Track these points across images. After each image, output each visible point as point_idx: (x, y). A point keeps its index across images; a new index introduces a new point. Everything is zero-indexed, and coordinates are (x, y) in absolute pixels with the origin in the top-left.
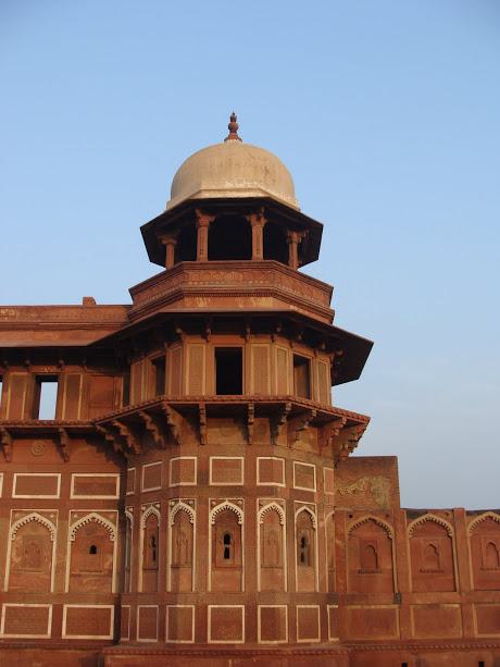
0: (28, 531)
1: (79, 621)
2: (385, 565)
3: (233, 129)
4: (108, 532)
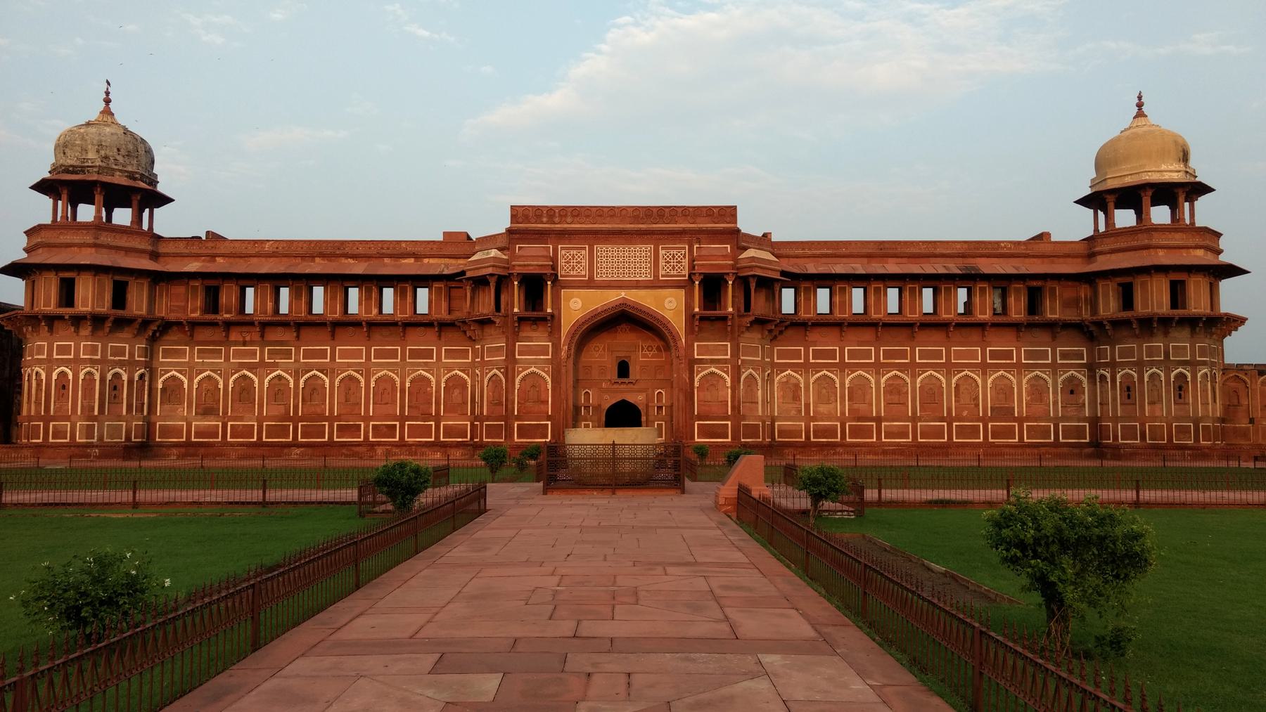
0: (1033, 382)
1: (1068, 432)
3: (1140, 105)
4: (1081, 382)
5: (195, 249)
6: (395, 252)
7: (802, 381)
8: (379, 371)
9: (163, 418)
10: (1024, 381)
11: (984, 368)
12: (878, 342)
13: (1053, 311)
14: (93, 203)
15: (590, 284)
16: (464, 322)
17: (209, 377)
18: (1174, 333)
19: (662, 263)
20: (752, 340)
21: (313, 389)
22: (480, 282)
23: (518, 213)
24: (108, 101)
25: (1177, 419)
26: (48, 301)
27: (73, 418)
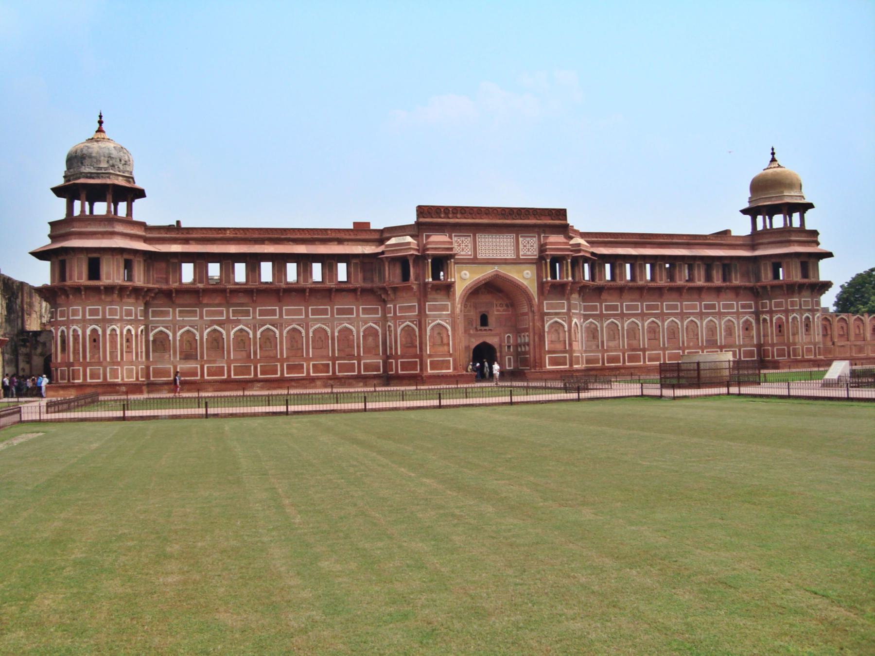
1: (747, 354)
2: (829, 333)
3: (773, 154)
4: (751, 323)
5: (174, 235)
6: (324, 237)
7: (599, 325)
8: (315, 325)
9: (155, 362)
11: (701, 315)
12: (641, 298)
13: (736, 280)
14: (104, 201)
15: (474, 261)
16: (384, 289)
17: (188, 331)
18: (804, 293)
19: (521, 246)
20: (575, 298)
21: (268, 339)
22: (393, 260)
23: (422, 211)
24: (100, 122)
25: (806, 344)
26: (79, 275)
27: (104, 364)
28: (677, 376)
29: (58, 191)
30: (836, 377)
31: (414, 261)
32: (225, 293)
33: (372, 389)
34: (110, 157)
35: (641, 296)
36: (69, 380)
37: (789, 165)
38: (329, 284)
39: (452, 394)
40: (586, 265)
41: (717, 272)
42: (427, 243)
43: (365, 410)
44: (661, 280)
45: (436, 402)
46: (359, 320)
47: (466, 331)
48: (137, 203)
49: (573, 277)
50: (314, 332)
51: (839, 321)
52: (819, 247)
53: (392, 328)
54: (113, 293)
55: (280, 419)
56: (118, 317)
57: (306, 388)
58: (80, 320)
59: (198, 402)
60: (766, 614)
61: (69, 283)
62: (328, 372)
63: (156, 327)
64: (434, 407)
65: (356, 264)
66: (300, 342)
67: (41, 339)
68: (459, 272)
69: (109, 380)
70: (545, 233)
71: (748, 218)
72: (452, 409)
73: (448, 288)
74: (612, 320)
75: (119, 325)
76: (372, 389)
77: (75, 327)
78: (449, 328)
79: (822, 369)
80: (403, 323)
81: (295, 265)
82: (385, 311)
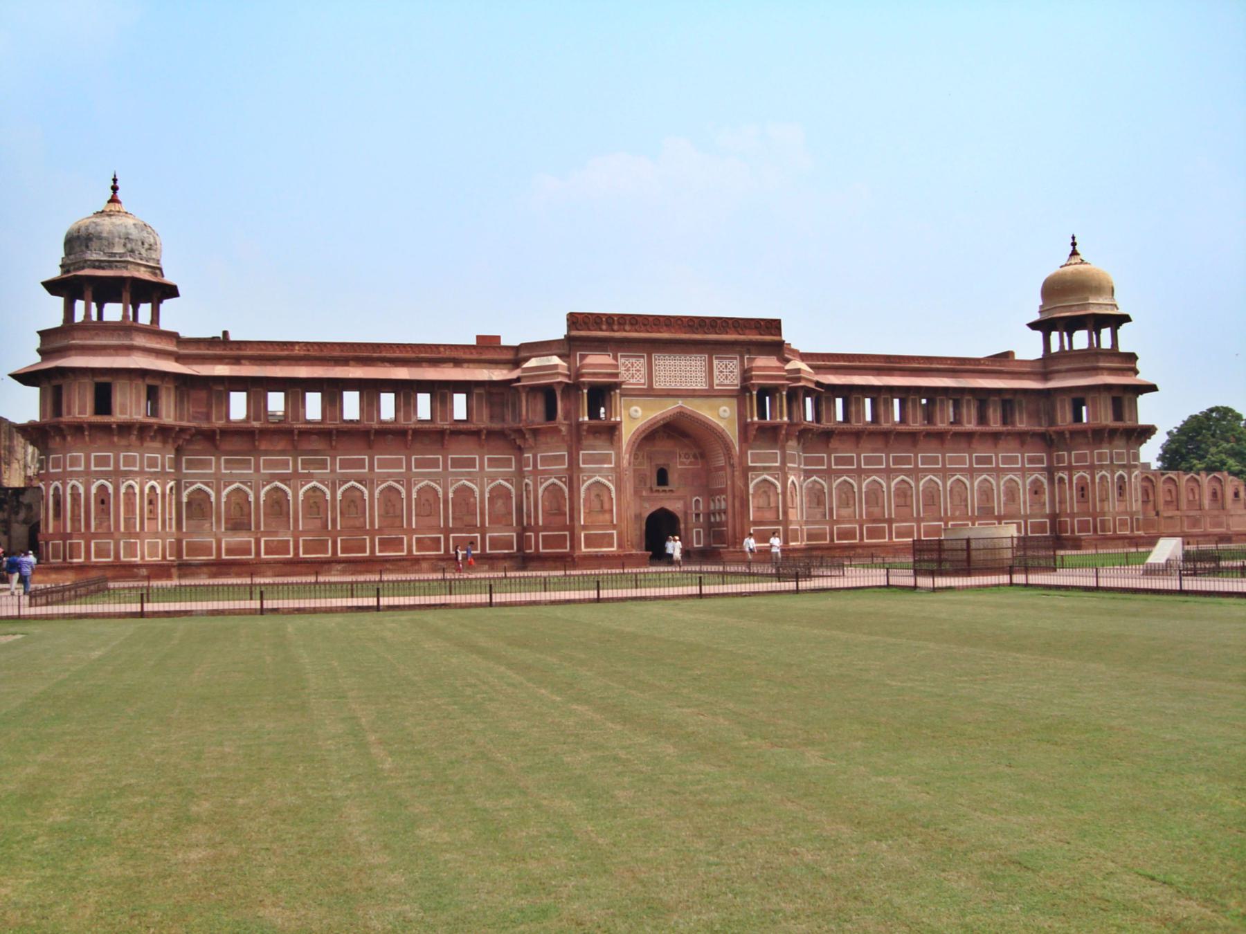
1: (1035, 527)
2: (1151, 498)
3: (1074, 244)
4: (1042, 483)
5: (218, 352)
10: (1002, 483)
11: (971, 472)
12: (887, 448)
13: (1021, 422)
15: (649, 392)
16: (520, 432)
17: (238, 489)
20: (793, 447)
21: (353, 502)
22: (534, 390)
23: (574, 320)
24: (115, 189)
26: (81, 408)
27: (117, 535)
28: (936, 557)
29: (52, 287)
30: (1163, 561)
31: (563, 391)
32: (291, 434)
33: (501, 574)
34: (128, 238)
35: (887, 443)
36: (65, 559)
37: (1096, 261)
38: (441, 424)
39: (616, 582)
40: (808, 400)
41: (995, 411)
42: (582, 367)
43: (491, 604)
44: (915, 421)
45: (592, 594)
46: (483, 476)
47: (637, 492)
48: (167, 306)
49: (790, 415)
50: (418, 492)
51: (1165, 482)
52: (1139, 377)
53: (531, 488)
54: (130, 434)
55: (367, 617)
56: (137, 469)
57: (407, 572)
58: (81, 472)
59: (250, 591)
60: (1082, 909)
61: (66, 418)
62: (439, 550)
63: (192, 484)
64: (590, 601)
65: (480, 396)
66: (398, 506)
67: (25, 499)
68: (628, 408)
69: (123, 558)
70: (749, 353)
71: (1038, 335)
72: (616, 604)
73: (611, 431)
74: (845, 478)
75: (138, 480)
76: (501, 574)
77: (74, 482)
78: (613, 488)
79: (1141, 550)
80: (546, 480)
81: (392, 396)
82: (521, 463)
